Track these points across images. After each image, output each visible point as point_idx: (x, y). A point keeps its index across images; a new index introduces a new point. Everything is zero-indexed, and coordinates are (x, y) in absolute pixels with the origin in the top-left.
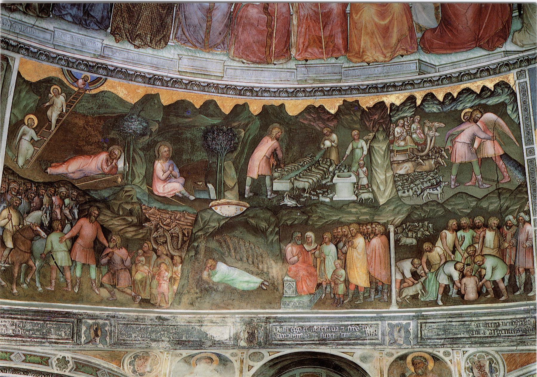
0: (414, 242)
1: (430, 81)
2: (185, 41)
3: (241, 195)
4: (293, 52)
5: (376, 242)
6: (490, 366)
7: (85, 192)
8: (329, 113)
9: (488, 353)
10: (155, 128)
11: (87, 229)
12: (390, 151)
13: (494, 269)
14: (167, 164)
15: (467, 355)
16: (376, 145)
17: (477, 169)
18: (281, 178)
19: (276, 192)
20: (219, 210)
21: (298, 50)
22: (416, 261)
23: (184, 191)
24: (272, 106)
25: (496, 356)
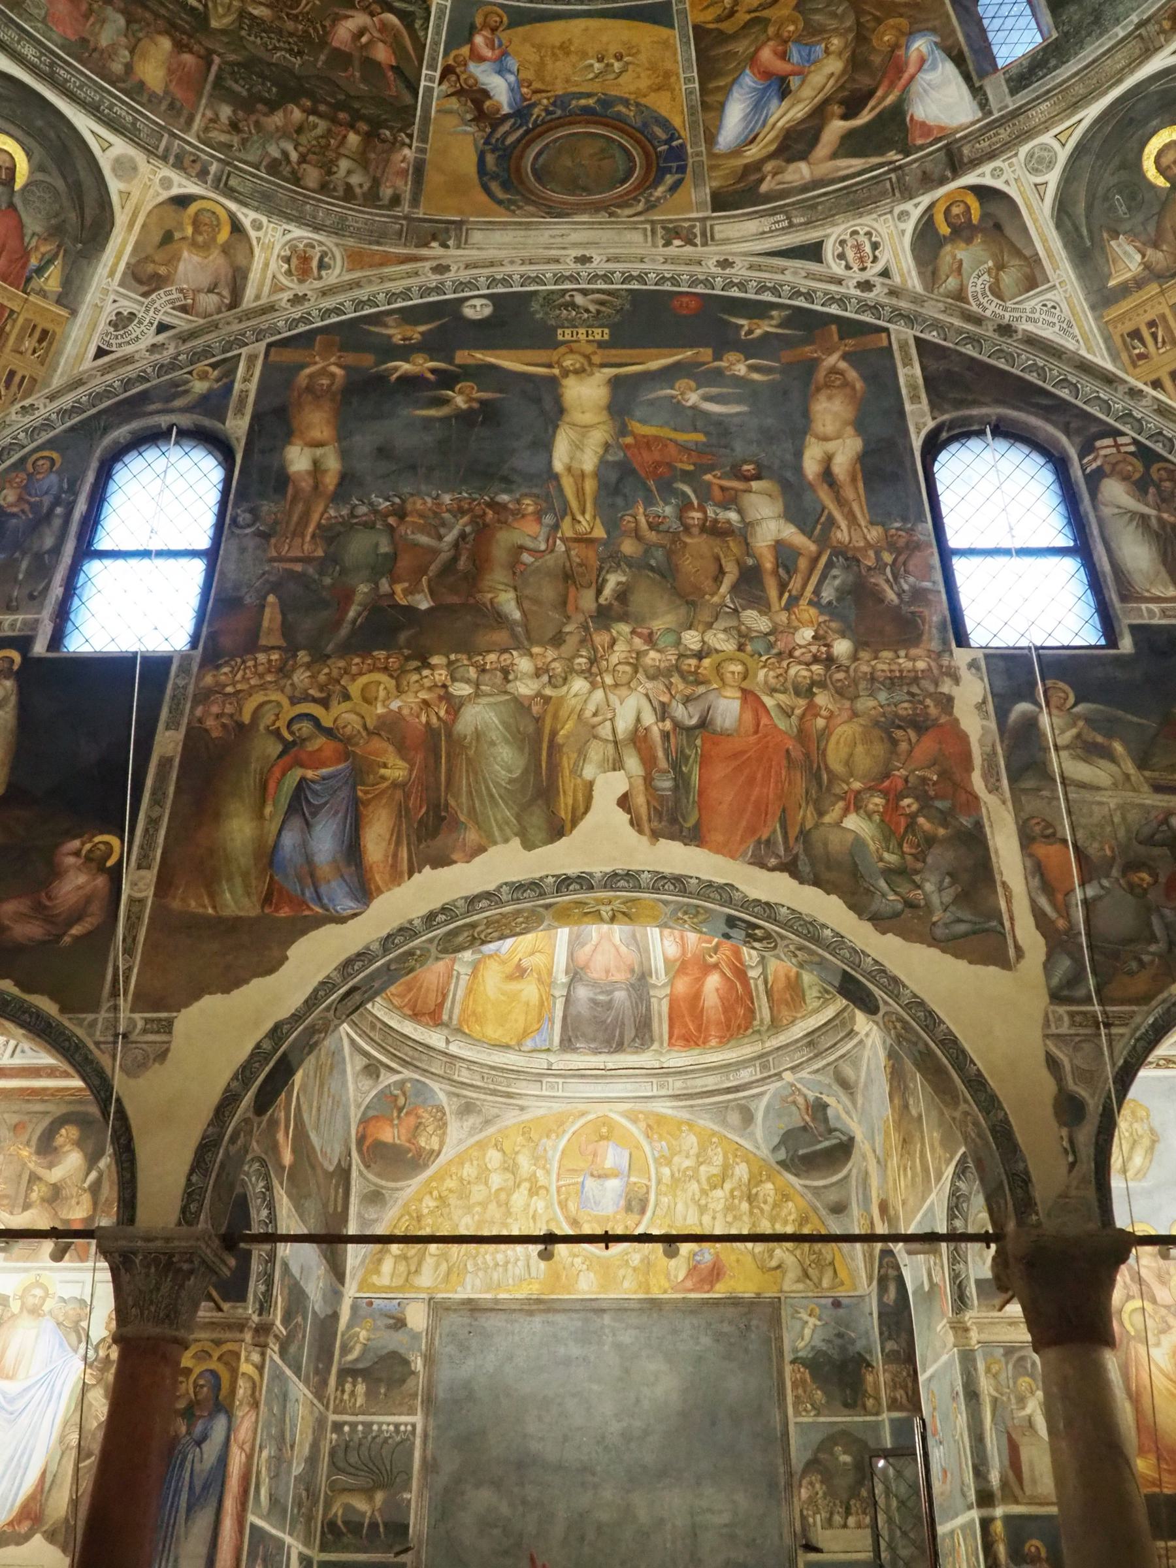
9: (321, 243)
13: (349, 172)
15: (288, 237)
17: (356, 63)
22: (241, 114)
25: (334, 249)
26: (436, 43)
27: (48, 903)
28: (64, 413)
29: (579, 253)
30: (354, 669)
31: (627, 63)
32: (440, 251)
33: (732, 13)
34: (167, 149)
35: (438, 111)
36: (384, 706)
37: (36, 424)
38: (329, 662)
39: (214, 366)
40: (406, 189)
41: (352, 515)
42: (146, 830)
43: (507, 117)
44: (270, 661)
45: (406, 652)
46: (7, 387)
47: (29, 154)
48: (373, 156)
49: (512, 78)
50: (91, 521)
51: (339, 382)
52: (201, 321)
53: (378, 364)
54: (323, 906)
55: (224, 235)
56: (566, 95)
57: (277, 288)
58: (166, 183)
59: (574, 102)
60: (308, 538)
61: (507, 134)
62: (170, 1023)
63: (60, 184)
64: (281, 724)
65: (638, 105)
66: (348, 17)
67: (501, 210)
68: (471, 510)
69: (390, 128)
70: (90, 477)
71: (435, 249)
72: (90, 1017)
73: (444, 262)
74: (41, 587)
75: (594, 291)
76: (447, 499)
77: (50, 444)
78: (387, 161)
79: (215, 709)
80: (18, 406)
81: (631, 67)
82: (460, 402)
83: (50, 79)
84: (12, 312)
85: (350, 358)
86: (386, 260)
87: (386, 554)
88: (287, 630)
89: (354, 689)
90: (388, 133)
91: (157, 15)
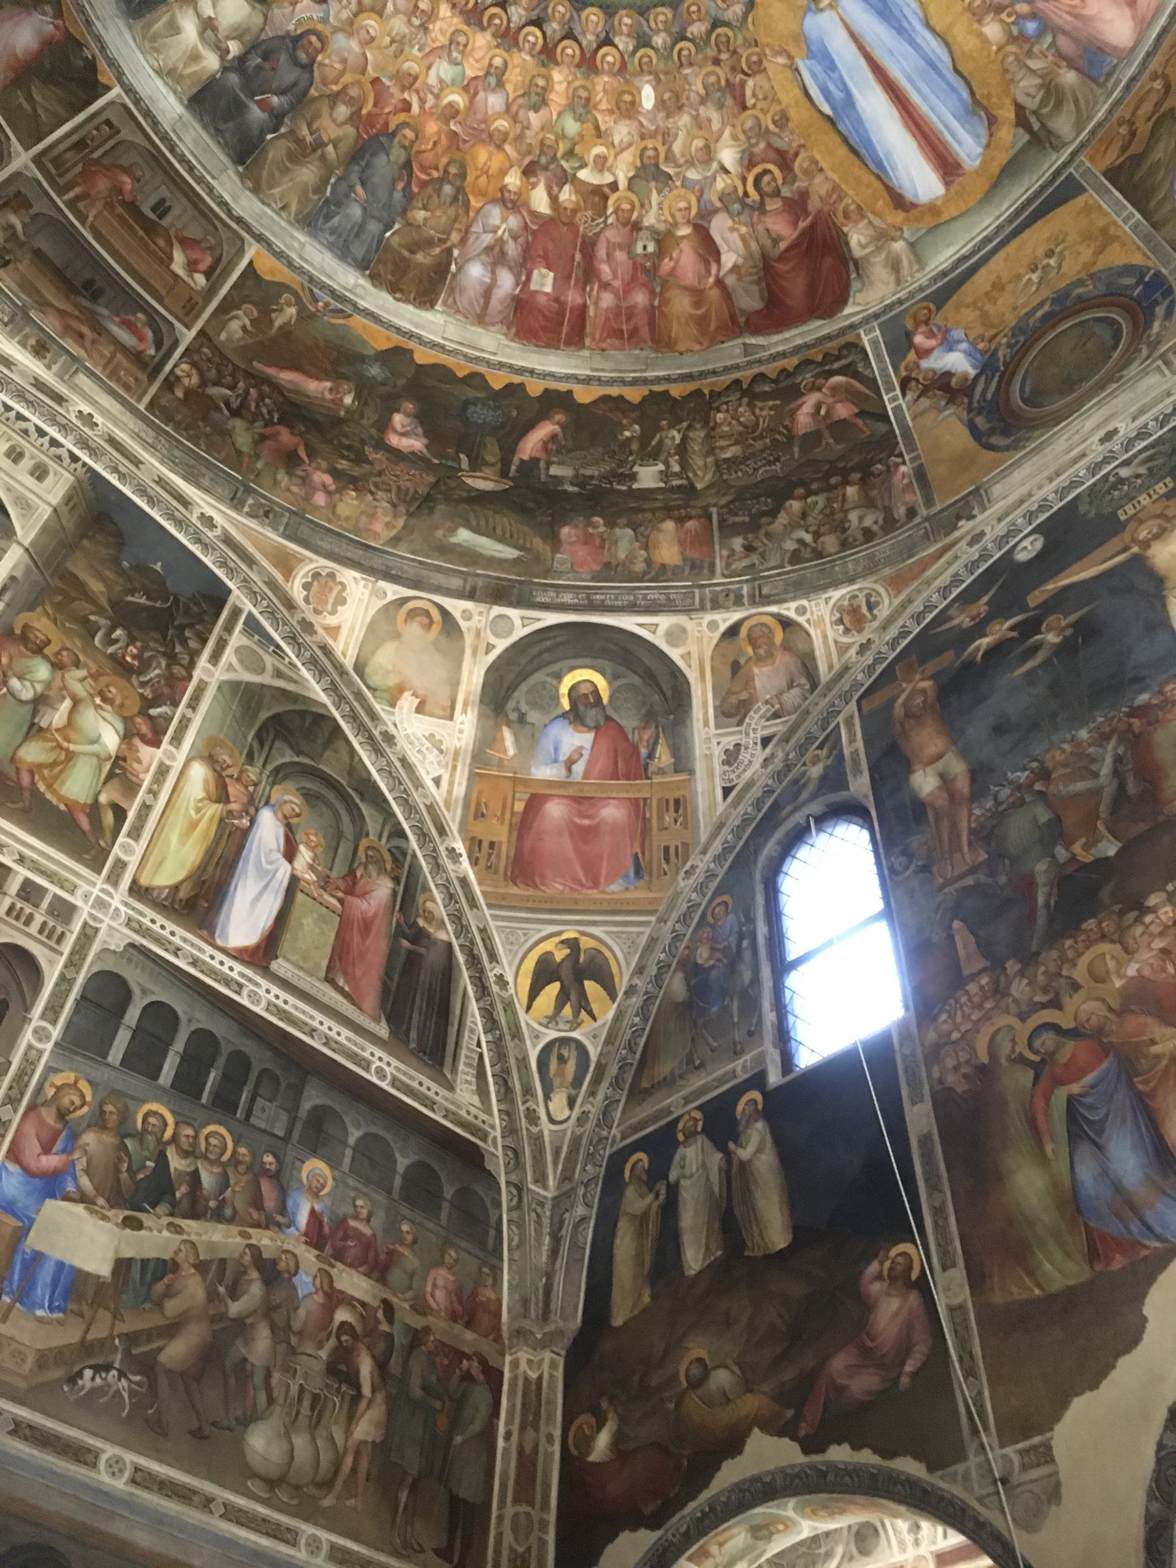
0: (747, 519)
1: (760, 361)
2: (454, 309)
3: (504, 473)
4: (588, 341)
5: (690, 524)
6: (868, 602)
7: (295, 405)
8: (628, 402)
9: (861, 589)
10: (401, 382)
11: (286, 437)
12: (709, 437)
14: (407, 420)
15: (832, 602)
16: (691, 434)
18: (561, 463)
19: (555, 477)
20: (469, 481)
21: (594, 339)
22: (750, 536)
23: (425, 451)
24: (557, 392)
26: (883, 370)
27: (870, 1344)
28: (718, 859)
29: (1102, 433)
30: (1070, 954)
31: (1061, 252)
32: (971, 523)
33: (1133, 134)
34: (702, 600)
35: (913, 419)
36: (1120, 977)
37: (701, 879)
38: (1041, 958)
39: (820, 747)
40: (917, 498)
41: (997, 803)
42: (936, 1223)
43: (977, 377)
44: (981, 987)
45: (1116, 908)
46: (667, 860)
47: (603, 673)
48: (874, 493)
49: (964, 346)
50: (776, 939)
51: (931, 694)
52: (794, 717)
53: (958, 656)
54: (1159, 1238)
55: (779, 636)
56: (1020, 319)
57: (843, 649)
58: (713, 625)
59: (1031, 321)
60: (966, 848)
61: (984, 391)
62: (1047, 1447)
63: (636, 680)
64: (1021, 1048)
65: (1092, 276)
66: (800, 406)
67: (1011, 452)
68: (1113, 731)
69: (879, 462)
70: (760, 900)
71: (965, 526)
72: (960, 1468)
73: (977, 531)
74: (754, 1021)
75: (1135, 456)
76: (1083, 734)
77: (718, 891)
78: (889, 489)
79: (950, 1063)
80: (682, 874)
81: (1066, 253)
82: (1052, 638)
83: (593, 607)
84: (645, 799)
85: (931, 667)
86: (925, 564)
87: (1049, 821)
88: (984, 947)
89: (1079, 973)
90: (879, 466)
91: (653, 511)
